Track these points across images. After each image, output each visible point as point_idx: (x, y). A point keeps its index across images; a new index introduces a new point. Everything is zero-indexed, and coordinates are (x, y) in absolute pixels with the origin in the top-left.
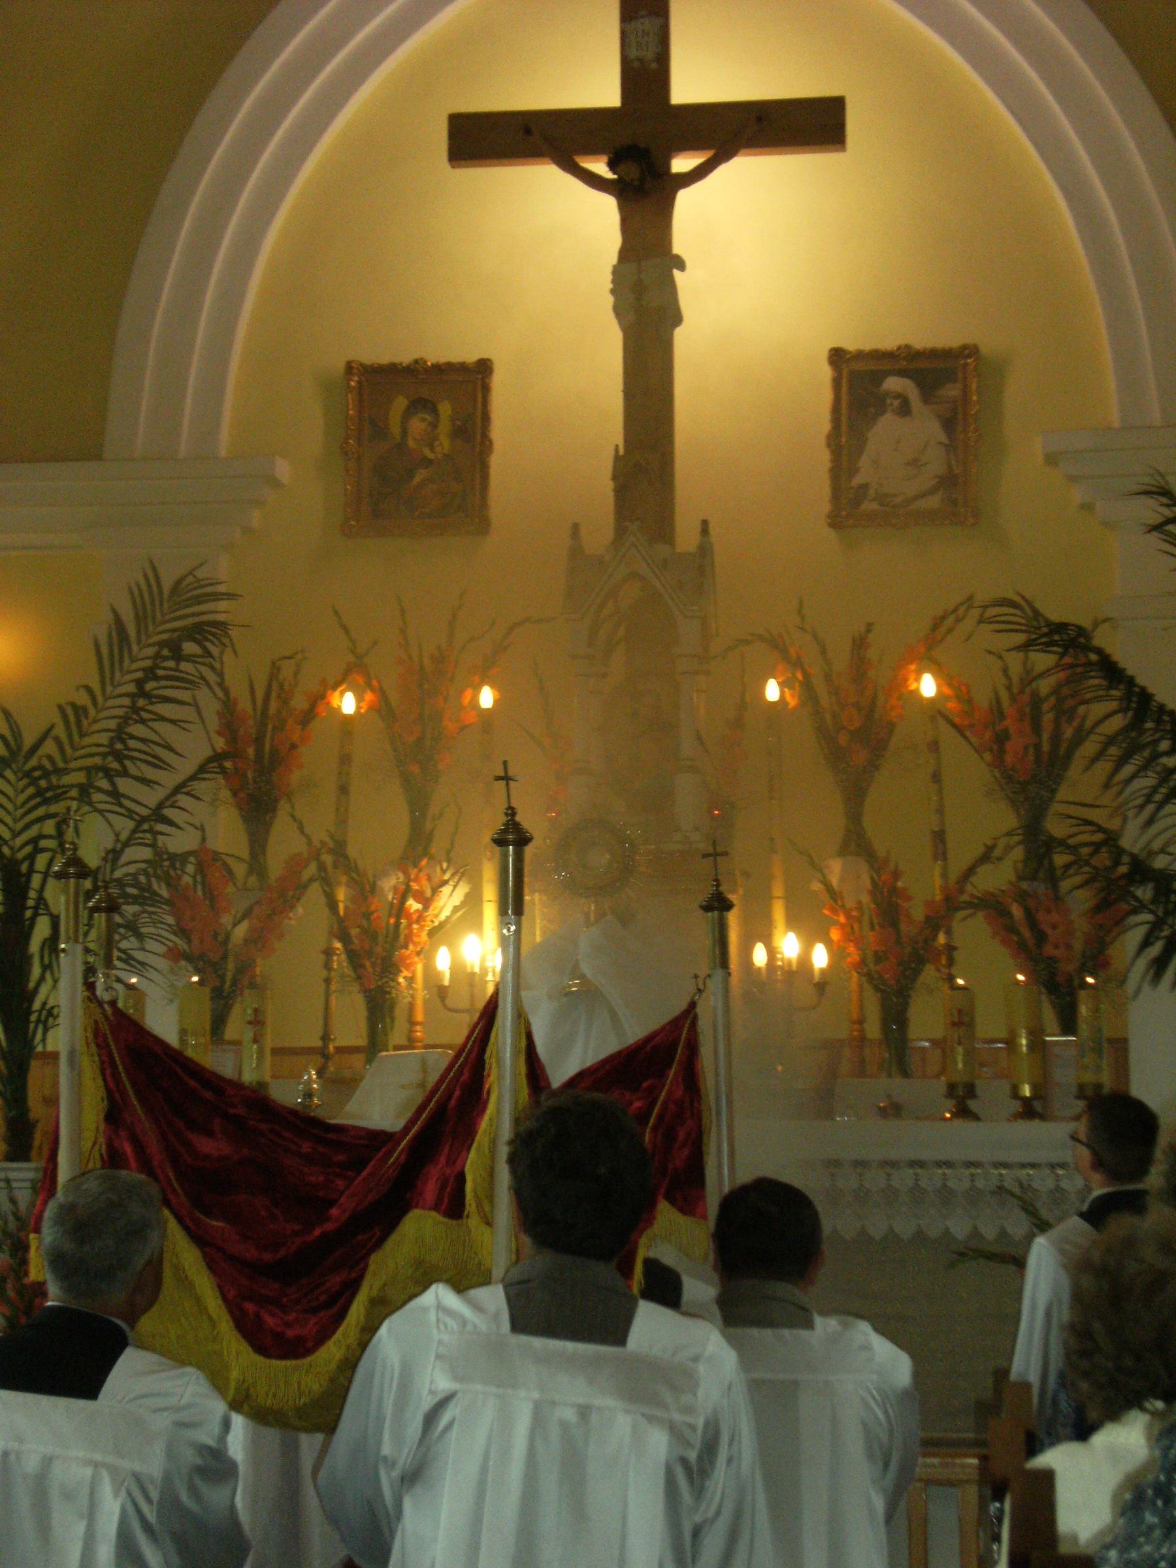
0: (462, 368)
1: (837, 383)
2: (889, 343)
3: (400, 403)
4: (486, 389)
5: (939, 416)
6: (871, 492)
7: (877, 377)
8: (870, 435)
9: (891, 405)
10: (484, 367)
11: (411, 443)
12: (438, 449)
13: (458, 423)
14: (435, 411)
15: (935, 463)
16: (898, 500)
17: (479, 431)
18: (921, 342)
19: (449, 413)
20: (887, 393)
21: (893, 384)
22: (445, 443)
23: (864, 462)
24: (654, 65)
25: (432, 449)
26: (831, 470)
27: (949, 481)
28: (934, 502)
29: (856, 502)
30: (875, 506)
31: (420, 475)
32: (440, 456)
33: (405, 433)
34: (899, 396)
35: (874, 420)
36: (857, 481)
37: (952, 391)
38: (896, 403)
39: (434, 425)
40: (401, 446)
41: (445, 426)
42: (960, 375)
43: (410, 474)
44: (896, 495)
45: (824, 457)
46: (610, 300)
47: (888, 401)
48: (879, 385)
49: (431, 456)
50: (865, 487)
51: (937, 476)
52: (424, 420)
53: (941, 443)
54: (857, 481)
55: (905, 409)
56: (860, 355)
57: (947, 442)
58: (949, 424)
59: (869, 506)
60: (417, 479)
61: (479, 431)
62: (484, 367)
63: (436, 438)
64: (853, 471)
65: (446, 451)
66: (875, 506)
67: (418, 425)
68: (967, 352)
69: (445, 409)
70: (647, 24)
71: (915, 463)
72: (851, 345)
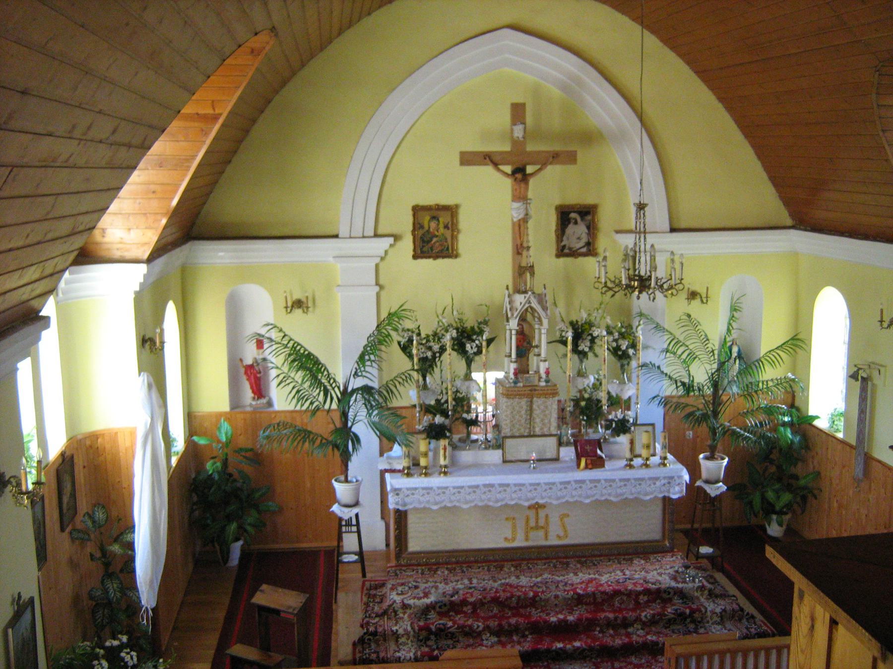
3: (428, 218)
6: (567, 248)
11: (431, 230)
14: (438, 220)
15: (585, 239)
16: (574, 249)
21: (573, 215)
23: (565, 238)
24: (522, 139)
25: (438, 232)
27: (588, 244)
28: (584, 250)
31: (435, 240)
33: (429, 228)
35: (567, 225)
36: (563, 244)
37: (589, 218)
38: (574, 221)
39: (438, 225)
40: (428, 231)
41: (441, 226)
43: (432, 240)
45: (553, 237)
49: (436, 233)
50: (564, 247)
57: (586, 231)
58: (588, 228)
59: (566, 251)
60: (433, 242)
63: (439, 229)
64: (562, 241)
67: (433, 225)
69: (441, 220)
71: (579, 238)
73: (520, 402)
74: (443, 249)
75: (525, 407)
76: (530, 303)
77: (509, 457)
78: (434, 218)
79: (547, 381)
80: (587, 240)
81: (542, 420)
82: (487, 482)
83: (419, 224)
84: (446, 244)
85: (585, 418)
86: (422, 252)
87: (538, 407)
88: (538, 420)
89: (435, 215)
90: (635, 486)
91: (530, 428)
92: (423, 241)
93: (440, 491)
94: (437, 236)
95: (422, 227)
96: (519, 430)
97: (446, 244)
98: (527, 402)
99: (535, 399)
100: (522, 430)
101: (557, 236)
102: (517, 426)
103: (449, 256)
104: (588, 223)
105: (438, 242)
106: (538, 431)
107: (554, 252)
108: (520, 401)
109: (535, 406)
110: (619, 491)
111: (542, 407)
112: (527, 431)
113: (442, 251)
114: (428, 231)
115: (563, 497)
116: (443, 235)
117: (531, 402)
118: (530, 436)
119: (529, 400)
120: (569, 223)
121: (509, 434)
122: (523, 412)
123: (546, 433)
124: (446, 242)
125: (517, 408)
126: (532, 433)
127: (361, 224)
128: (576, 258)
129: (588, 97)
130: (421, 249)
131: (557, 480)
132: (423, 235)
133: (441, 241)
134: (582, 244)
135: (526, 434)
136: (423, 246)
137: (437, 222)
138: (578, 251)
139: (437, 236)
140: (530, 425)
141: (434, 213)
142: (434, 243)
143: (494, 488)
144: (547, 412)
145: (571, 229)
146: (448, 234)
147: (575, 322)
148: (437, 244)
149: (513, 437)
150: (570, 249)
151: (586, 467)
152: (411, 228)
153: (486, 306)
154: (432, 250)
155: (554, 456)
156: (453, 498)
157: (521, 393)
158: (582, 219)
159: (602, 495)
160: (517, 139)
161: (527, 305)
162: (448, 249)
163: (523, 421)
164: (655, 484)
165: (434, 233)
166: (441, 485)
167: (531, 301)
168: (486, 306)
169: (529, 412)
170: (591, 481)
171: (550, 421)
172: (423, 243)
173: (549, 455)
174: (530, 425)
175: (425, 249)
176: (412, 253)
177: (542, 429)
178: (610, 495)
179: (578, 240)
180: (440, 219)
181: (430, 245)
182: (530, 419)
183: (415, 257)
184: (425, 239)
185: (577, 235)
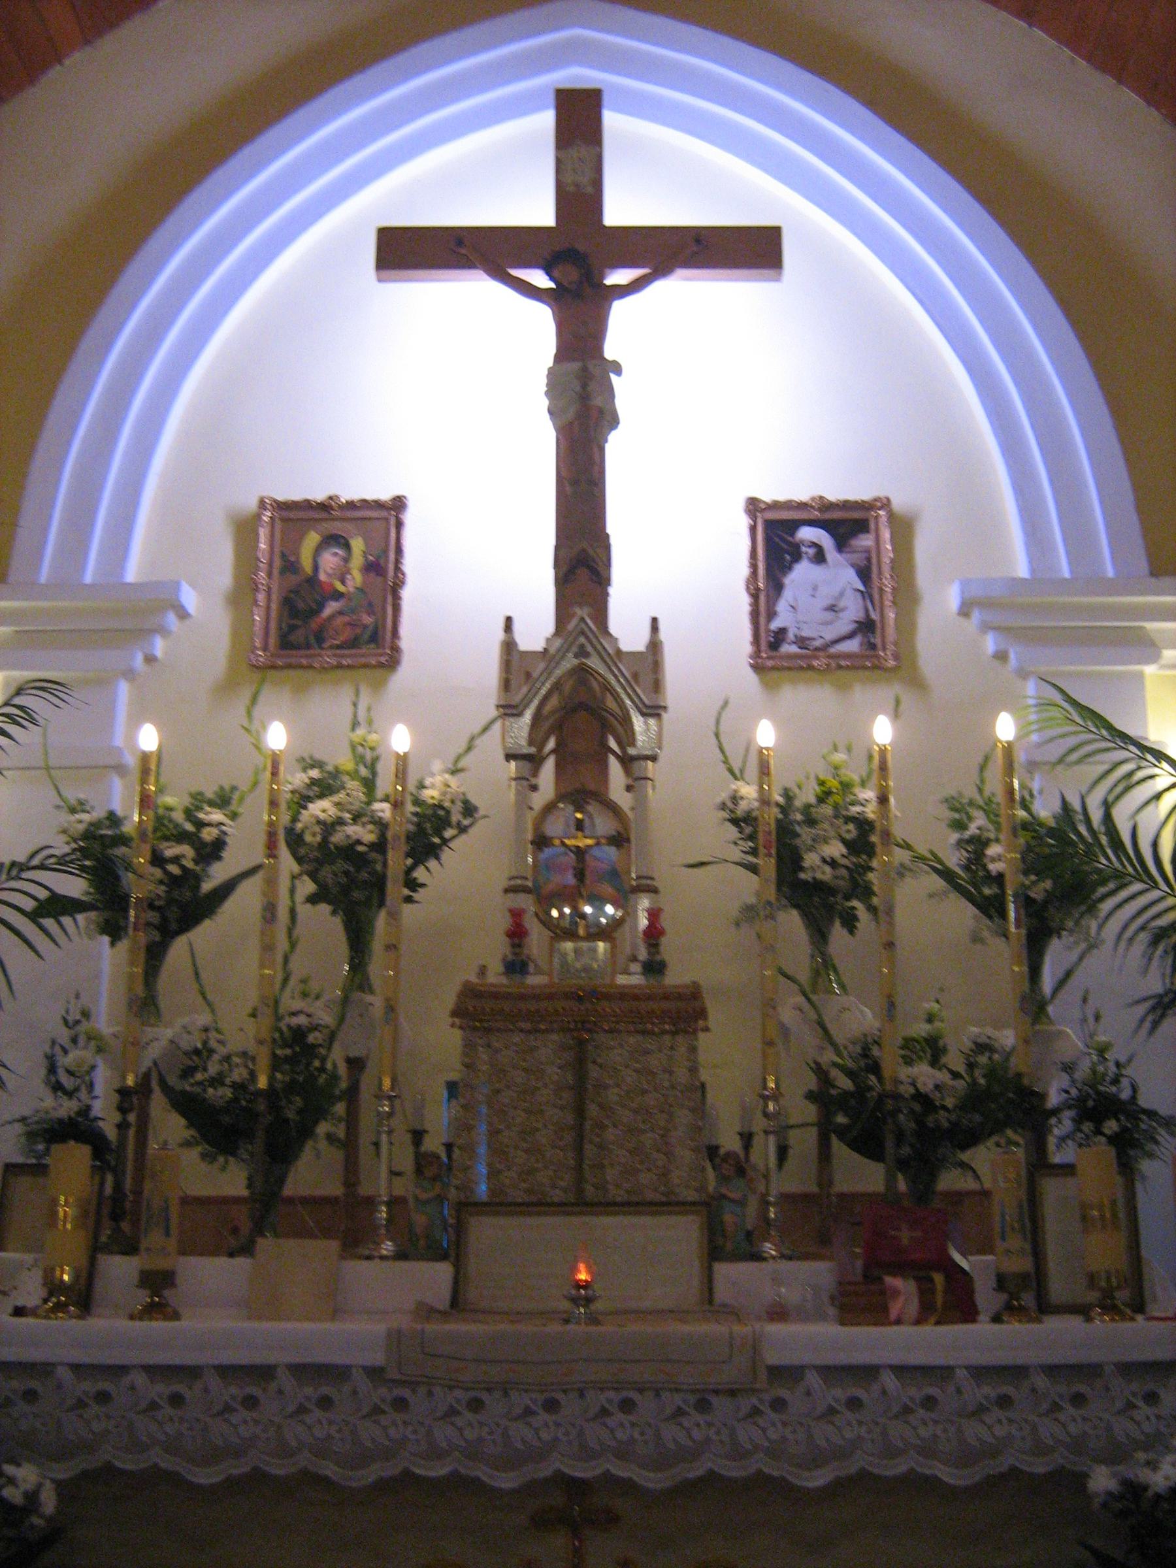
0: (378, 505)
1: (753, 529)
2: (802, 494)
3: (313, 539)
4: (399, 525)
5: (853, 566)
6: (791, 636)
7: (795, 525)
10: (398, 504)
11: (322, 577)
12: (349, 583)
14: (347, 546)
15: (853, 610)
16: (818, 643)
17: (391, 566)
18: (834, 494)
19: (363, 548)
20: (802, 542)
21: (806, 534)
22: (356, 578)
23: (782, 606)
25: (343, 582)
27: (866, 627)
28: (853, 646)
29: (775, 646)
30: (794, 649)
31: (332, 607)
32: (351, 589)
33: (316, 568)
35: (790, 568)
36: (775, 625)
37: (865, 541)
38: (811, 551)
39: (346, 560)
40: (312, 581)
41: (357, 561)
42: (872, 526)
43: (321, 606)
44: (813, 639)
46: (545, 403)
47: (804, 549)
48: (792, 534)
50: (782, 631)
52: (336, 554)
55: (820, 557)
56: (775, 506)
57: (862, 588)
58: (864, 573)
59: (788, 648)
61: (391, 566)
62: (398, 504)
63: (348, 572)
64: (771, 615)
66: (794, 649)
67: (330, 560)
68: (879, 504)
69: (357, 545)
71: (832, 608)
72: (767, 496)
73: (533, 1050)
74: (356, 639)
80: (860, 616)
90: (1056, 1407)
91: (579, 1168)
93: (88, 1387)
94: (338, 596)
101: (755, 595)
105: (341, 613)
110: (974, 1431)
120: (797, 557)
123: (650, 1196)
134: (844, 624)
135: (557, 1196)
136: (292, 628)
137: (340, 552)
143: (347, 1388)
145: (802, 573)
148: (340, 620)
150: (801, 642)
158: (841, 544)
161: (570, 662)
164: (1152, 1398)
165: (331, 585)
175: (298, 636)
178: (928, 1450)
179: (829, 616)
181: (314, 624)
184: (301, 605)
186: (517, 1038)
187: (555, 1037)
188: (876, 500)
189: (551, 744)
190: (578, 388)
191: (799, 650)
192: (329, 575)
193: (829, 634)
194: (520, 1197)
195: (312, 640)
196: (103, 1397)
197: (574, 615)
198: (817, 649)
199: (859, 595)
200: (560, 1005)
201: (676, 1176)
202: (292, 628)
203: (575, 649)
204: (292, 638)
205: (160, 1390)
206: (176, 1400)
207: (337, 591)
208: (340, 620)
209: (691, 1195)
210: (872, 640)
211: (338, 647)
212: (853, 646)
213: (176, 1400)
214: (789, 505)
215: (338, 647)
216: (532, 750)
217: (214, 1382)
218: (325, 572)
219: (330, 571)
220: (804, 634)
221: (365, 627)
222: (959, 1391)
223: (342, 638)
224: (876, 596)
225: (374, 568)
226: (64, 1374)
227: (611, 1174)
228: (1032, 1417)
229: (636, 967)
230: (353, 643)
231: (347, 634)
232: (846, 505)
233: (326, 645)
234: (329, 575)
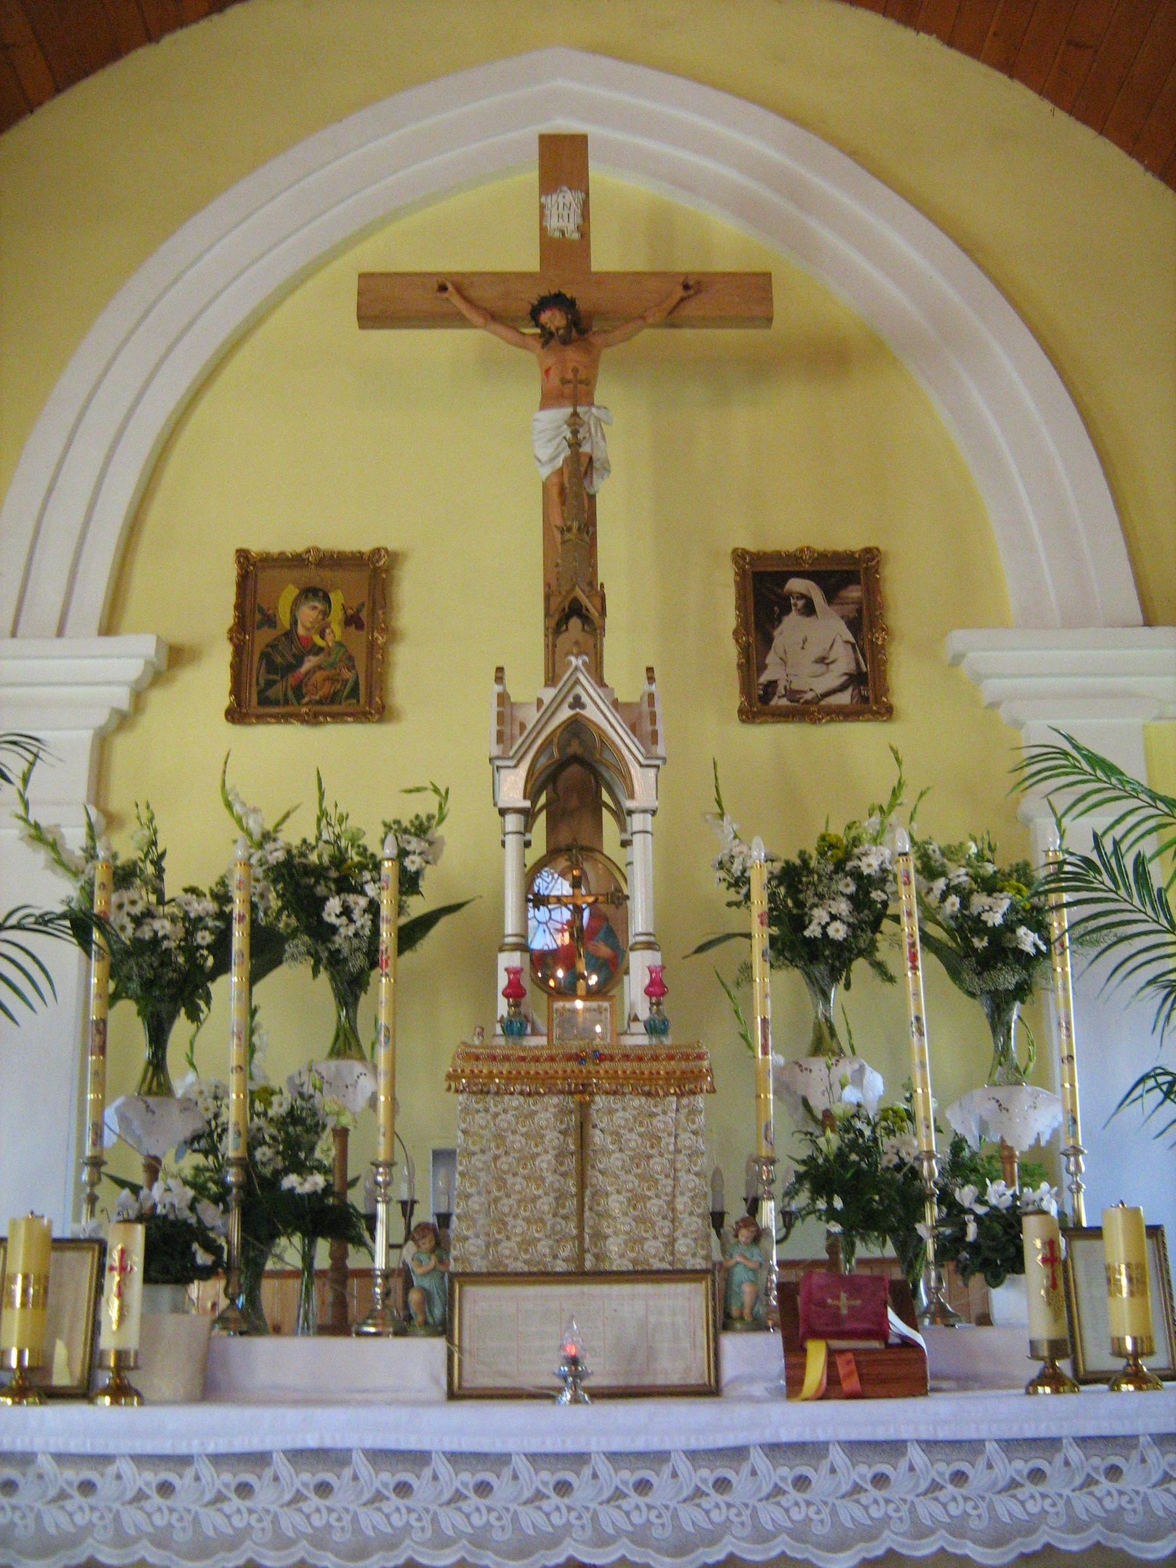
3: (290, 593)
5: (842, 617)
6: (781, 690)
8: (776, 633)
9: (796, 605)
11: (301, 631)
12: (329, 637)
13: (350, 612)
14: (327, 599)
15: (844, 662)
16: (809, 696)
20: (791, 594)
21: (796, 585)
23: (771, 659)
25: (323, 637)
26: (740, 666)
27: (856, 679)
28: (844, 698)
30: (784, 702)
31: (310, 662)
33: (294, 622)
34: (802, 596)
35: (780, 621)
36: (764, 679)
37: (854, 593)
38: (800, 603)
39: (326, 614)
40: (290, 635)
41: (336, 615)
43: (300, 661)
44: (805, 692)
45: (731, 652)
47: (792, 601)
50: (772, 684)
51: (846, 674)
52: (315, 608)
53: (847, 642)
54: (764, 679)
55: (809, 609)
57: (853, 640)
58: (854, 625)
59: (781, 702)
63: (328, 626)
64: (762, 667)
65: (338, 638)
66: (784, 702)
67: (308, 614)
69: (337, 598)
70: (567, 198)
71: (822, 660)
73: (533, 1114)
74: (336, 694)
75: (552, 1137)
76: (577, 703)
77: (478, 1377)
78: (310, 592)
79: (655, 1028)
80: (852, 667)
81: (636, 1200)
82: (311, 1441)
83: (261, 610)
84: (347, 675)
85: (838, 1203)
86: (264, 701)
87: (617, 1136)
88: (615, 1203)
89: (316, 582)
90: (1090, 1481)
91: (580, 1237)
92: (271, 667)
93: (72, 1475)
95: (270, 621)
96: (527, 1243)
97: (347, 675)
98: (563, 1112)
99: (600, 1101)
100: (543, 1247)
101: (745, 651)
102: (520, 1226)
103: (362, 716)
104: (851, 610)
105: (320, 667)
106: (617, 1254)
107: (735, 700)
108: (530, 1104)
109: (597, 1138)
110: (1006, 1507)
111: (633, 1140)
112: (567, 1250)
113: (333, 699)
114: (290, 635)
115: (712, 1538)
116: (340, 644)
117: (584, 1109)
118: (578, 1275)
119: (571, 1102)
120: (786, 610)
121: (479, 1265)
122: (545, 1162)
123: (657, 1265)
124: (352, 668)
125: (518, 1141)
126: (588, 1265)
127: (57, 599)
128: (815, 721)
129: (828, 236)
130: (260, 693)
131: (675, 1442)
132: (273, 646)
133: (333, 666)
134: (833, 679)
135: (560, 1266)
136: (270, 684)
138: (823, 703)
139: (320, 650)
140: (581, 1227)
141: (312, 576)
142: (308, 673)
143: (347, 1473)
144: (657, 1164)
146: (357, 642)
147: (798, 862)
148: (319, 676)
149: (497, 1276)
150: (792, 694)
151: (832, 1389)
152: (228, 618)
153: (436, 790)
154: (299, 695)
155: (698, 1375)
156: (132, 1517)
157: (533, 1068)
158: (831, 596)
159: (921, 1532)
160: (557, 234)
161: (565, 713)
162: (354, 692)
163: (545, 1204)
165: (309, 640)
166: (75, 1446)
167: (585, 699)
168: (436, 790)
169: (571, 1163)
170: (856, 1448)
171: (671, 1204)
172: (268, 672)
173: (670, 1372)
174: (581, 1227)
175: (276, 692)
176: (225, 700)
177: (635, 1241)
178: (958, 1529)
179: (819, 668)
180: (332, 596)
181: (291, 680)
182: (581, 1195)
183: (236, 714)
184: (279, 660)
185: (815, 651)
186: (516, 1101)
187: (555, 1100)
188: (868, 550)
189: (543, 800)
190: (569, 436)
191: (788, 703)
192: (308, 629)
193: (822, 685)
194: (520, 1266)
195: (290, 694)
196: (87, 1487)
197: (570, 663)
198: (807, 702)
199: (849, 647)
200: (559, 1066)
201: (682, 1246)
202: (270, 684)
203: (570, 699)
204: (270, 693)
205: (150, 1478)
206: (166, 1489)
207: (315, 645)
208: (319, 676)
209: (699, 1264)
210: (864, 693)
211: (320, 702)
212: (844, 698)
213: (166, 1489)
214: (778, 556)
215: (320, 702)
216: (527, 804)
217: (206, 1470)
218: (304, 626)
219: (309, 625)
220: (794, 686)
221: (347, 681)
222: (990, 1466)
223: (321, 693)
224: (867, 647)
225: (352, 621)
226: (45, 1463)
227: (614, 1246)
228: (1066, 1492)
229: (639, 1027)
230: (333, 699)
231: (326, 690)
232: (837, 557)
233: (306, 700)
234: (308, 629)
